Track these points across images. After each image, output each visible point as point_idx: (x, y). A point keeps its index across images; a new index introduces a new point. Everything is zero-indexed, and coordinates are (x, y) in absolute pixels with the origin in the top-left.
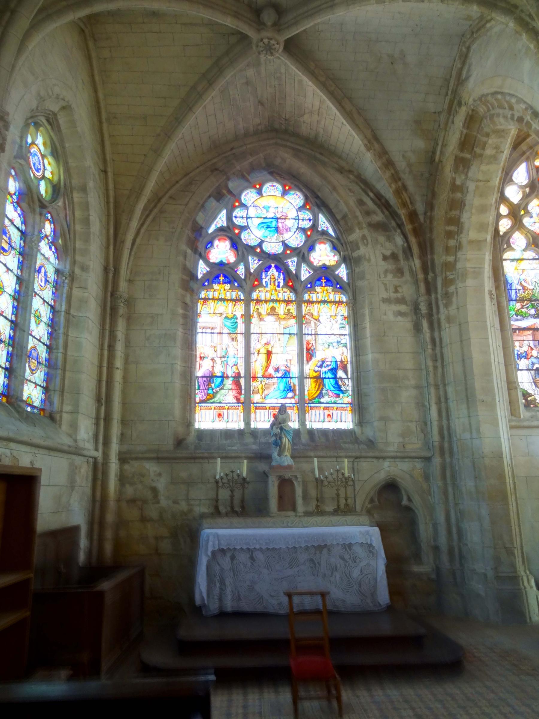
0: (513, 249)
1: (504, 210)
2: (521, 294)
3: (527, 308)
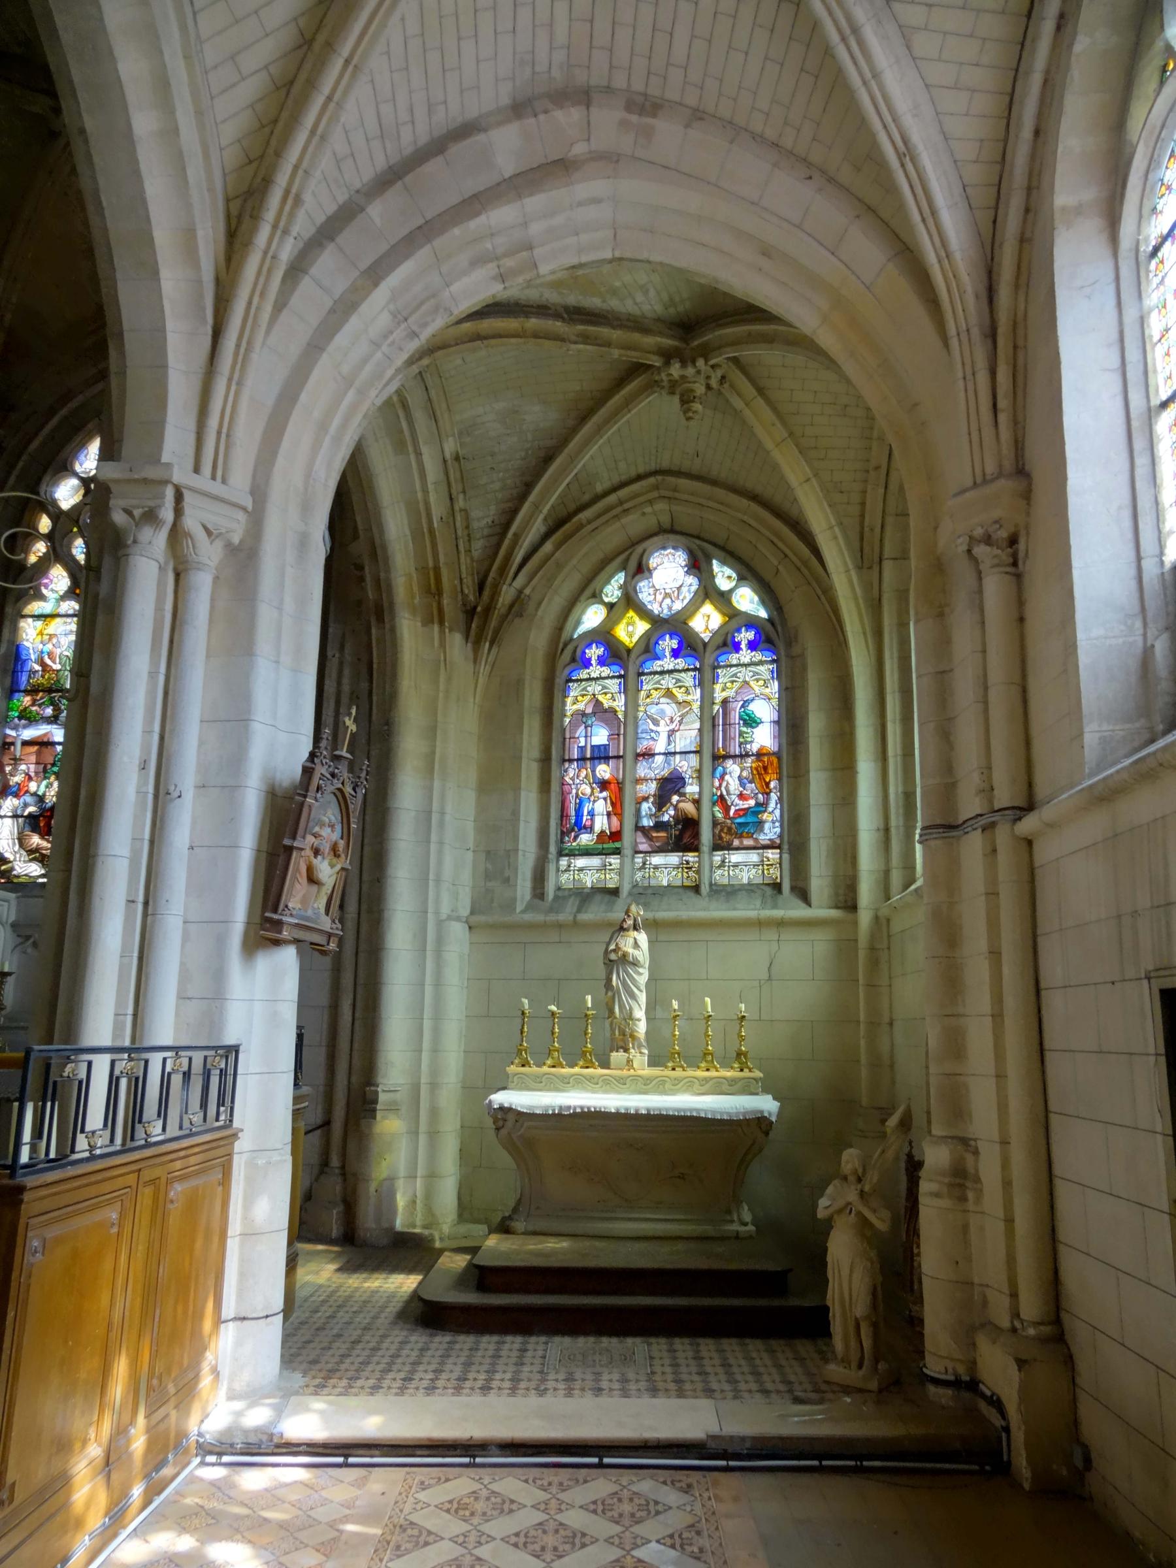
0: (42, 598)
1: (45, 524)
2: (38, 679)
3: (40, 706)
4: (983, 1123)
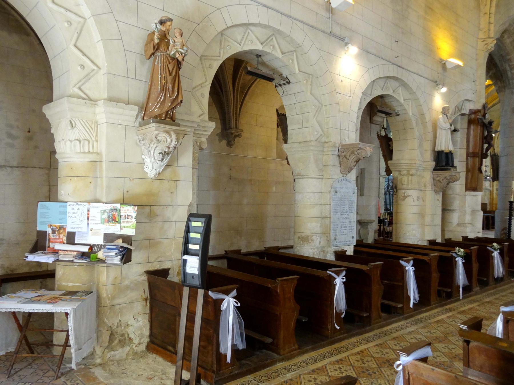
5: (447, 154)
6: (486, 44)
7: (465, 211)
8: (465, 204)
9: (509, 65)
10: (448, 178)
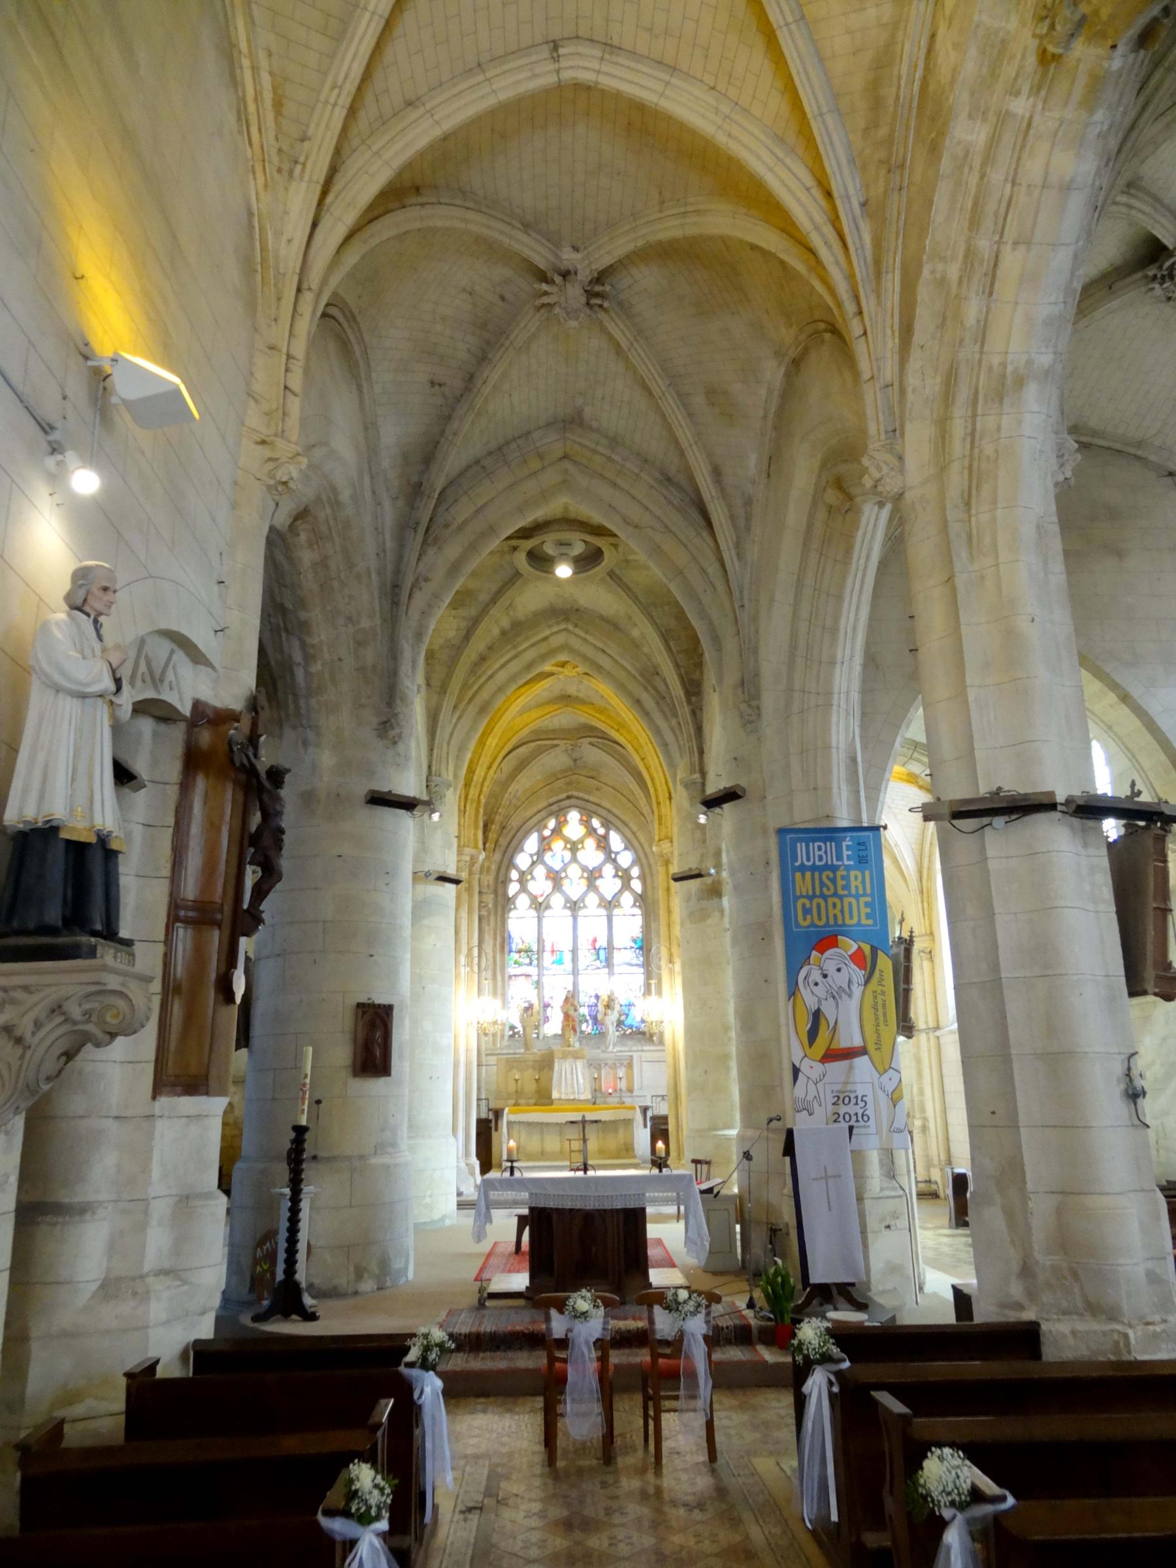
2: (521, 946)
4: (930, 1113)
5: (77, 849)
6: (270, 459)
7: (144, 1202)
8: (146, 1169)
9: (303, 645)
10: (76, 1012)
